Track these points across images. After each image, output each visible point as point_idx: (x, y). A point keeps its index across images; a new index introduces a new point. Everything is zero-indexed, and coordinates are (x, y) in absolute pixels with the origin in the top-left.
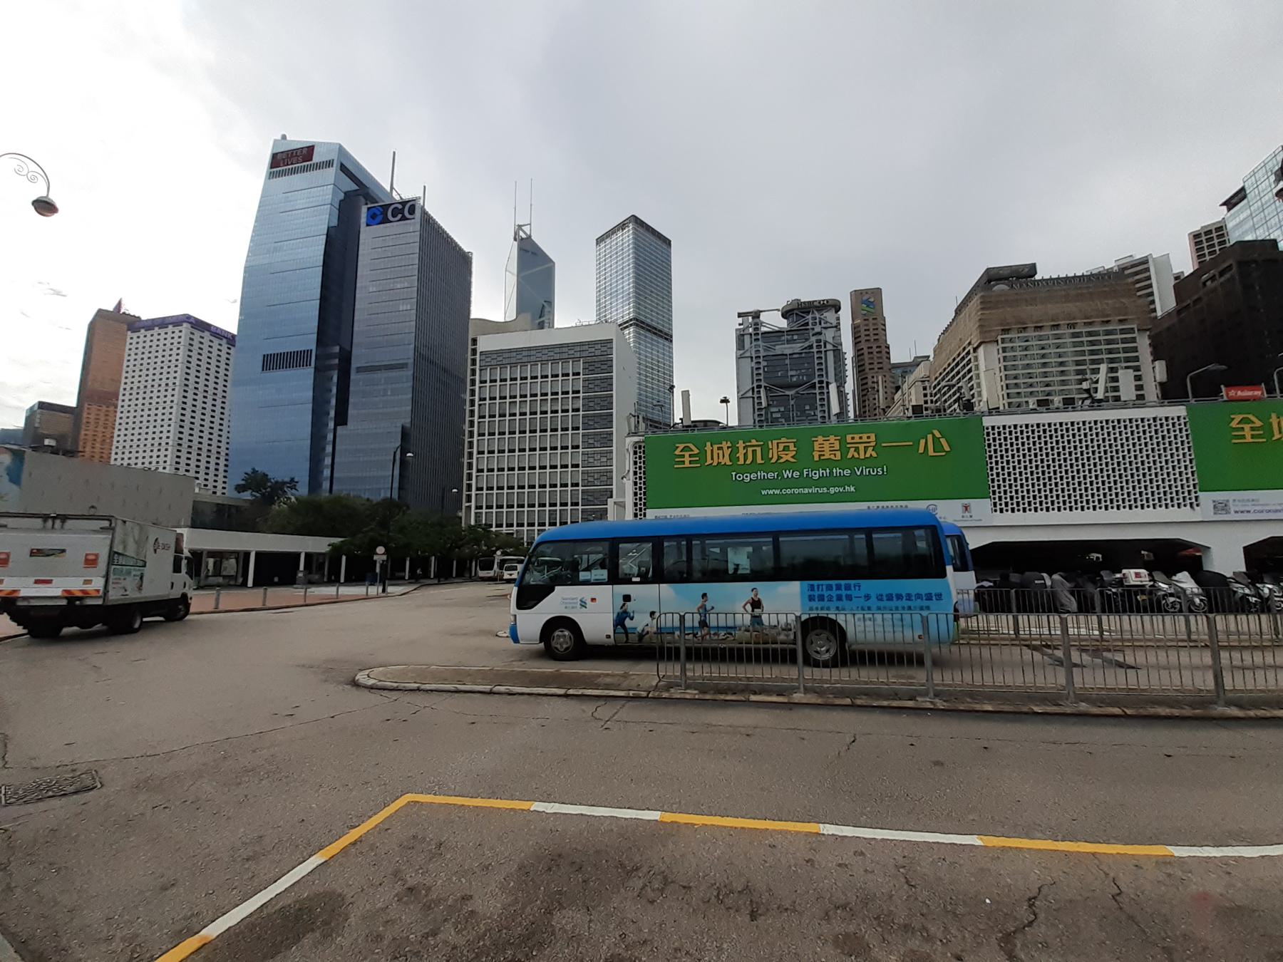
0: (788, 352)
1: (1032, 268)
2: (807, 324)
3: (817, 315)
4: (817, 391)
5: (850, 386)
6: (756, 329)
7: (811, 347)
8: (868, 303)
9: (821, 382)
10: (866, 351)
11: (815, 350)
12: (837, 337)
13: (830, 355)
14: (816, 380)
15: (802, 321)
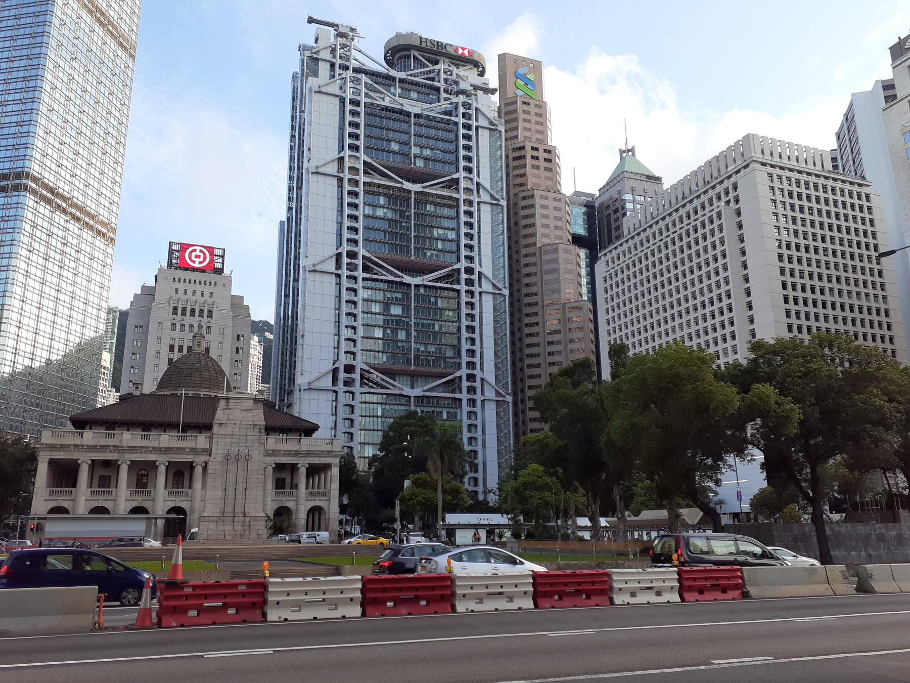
10: (529, 153)
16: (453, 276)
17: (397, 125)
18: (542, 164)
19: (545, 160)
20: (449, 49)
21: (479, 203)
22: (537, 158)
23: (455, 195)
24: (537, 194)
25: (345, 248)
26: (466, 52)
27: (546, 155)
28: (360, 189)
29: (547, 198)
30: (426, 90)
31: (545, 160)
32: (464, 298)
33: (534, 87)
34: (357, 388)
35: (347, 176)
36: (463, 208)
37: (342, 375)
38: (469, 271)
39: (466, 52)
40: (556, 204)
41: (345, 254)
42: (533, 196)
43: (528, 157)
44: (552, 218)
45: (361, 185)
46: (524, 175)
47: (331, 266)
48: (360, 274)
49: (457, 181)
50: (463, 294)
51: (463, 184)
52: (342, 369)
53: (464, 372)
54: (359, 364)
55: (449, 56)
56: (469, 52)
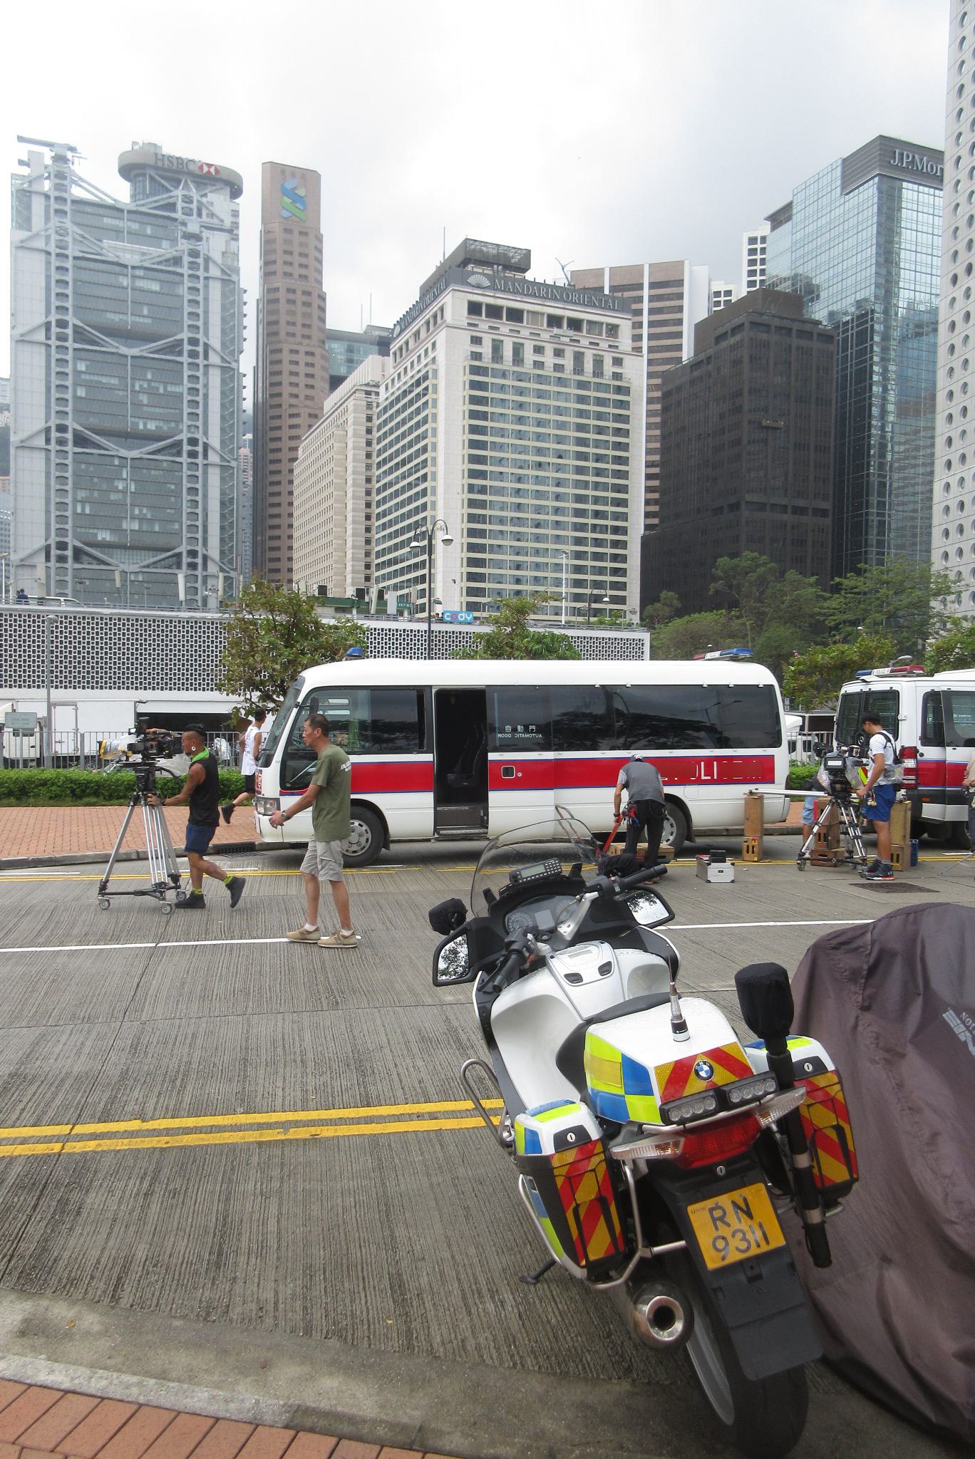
0: (129, 259)
1: (521, 262)
2: (171, 207)
3: (194, 193)
4: (185, 359)
5: (248, 362)
6: (58, 187)
7: (177, 261)
8: (296, 198)
9: (193, 342)
10: (282, 295)
11: (185, 270)
12: (231, 256)
13: (215, 290)
14: (185, 335)
15: (162, 198)
16: (176, 448)
17: (112, 280)
18: (300, 309)
19: (304, 304)
20: (192, 167)
21: (206, 366)
22: (294, 302)
23: (179, 359)
24: (286, 348)
25: (53, 422)
26: (212, 170)
27: (305, 298)
28: (69, 357)
29: (297, 352)
30: (160, 222)
31: (304, 304)
32: (186, 472)
33: (303, 203)
34: (70, 564)
35: (53, 342)
36: (186, 373)
37: (54, 552)
38: (193, 442)
39: (212, 170)
40: (309, 359)
41: (53, 429)
42: (280, 351)
43: (283, 301)
44: (302, 374)
45: (70, 351)
46: (276, 323)
47: (41, 442)
48: (70, 448)
49: (182, 340)
50: (185, 466)
51: (187, 347)
52: (53, 546)
53: (183, 549)
54: (71, 540)
55: (190, 174)
56: (216, 170)
